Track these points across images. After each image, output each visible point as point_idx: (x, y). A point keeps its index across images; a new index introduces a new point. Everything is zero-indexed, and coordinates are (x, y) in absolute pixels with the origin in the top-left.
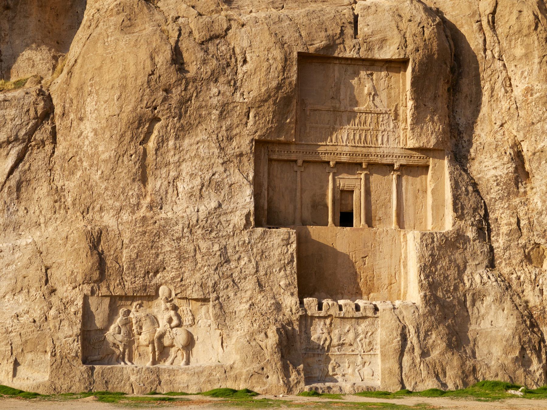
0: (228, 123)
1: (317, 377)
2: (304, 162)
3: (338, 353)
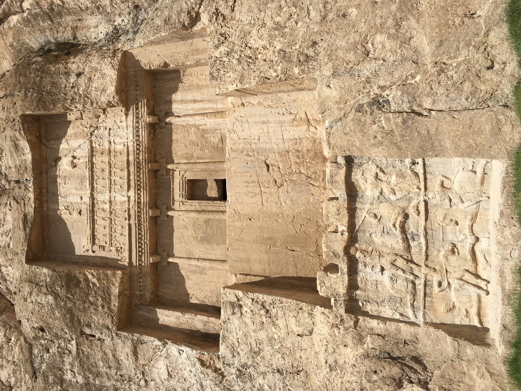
0: (101, 364)
2: (155, 252)
3: (423, 240)
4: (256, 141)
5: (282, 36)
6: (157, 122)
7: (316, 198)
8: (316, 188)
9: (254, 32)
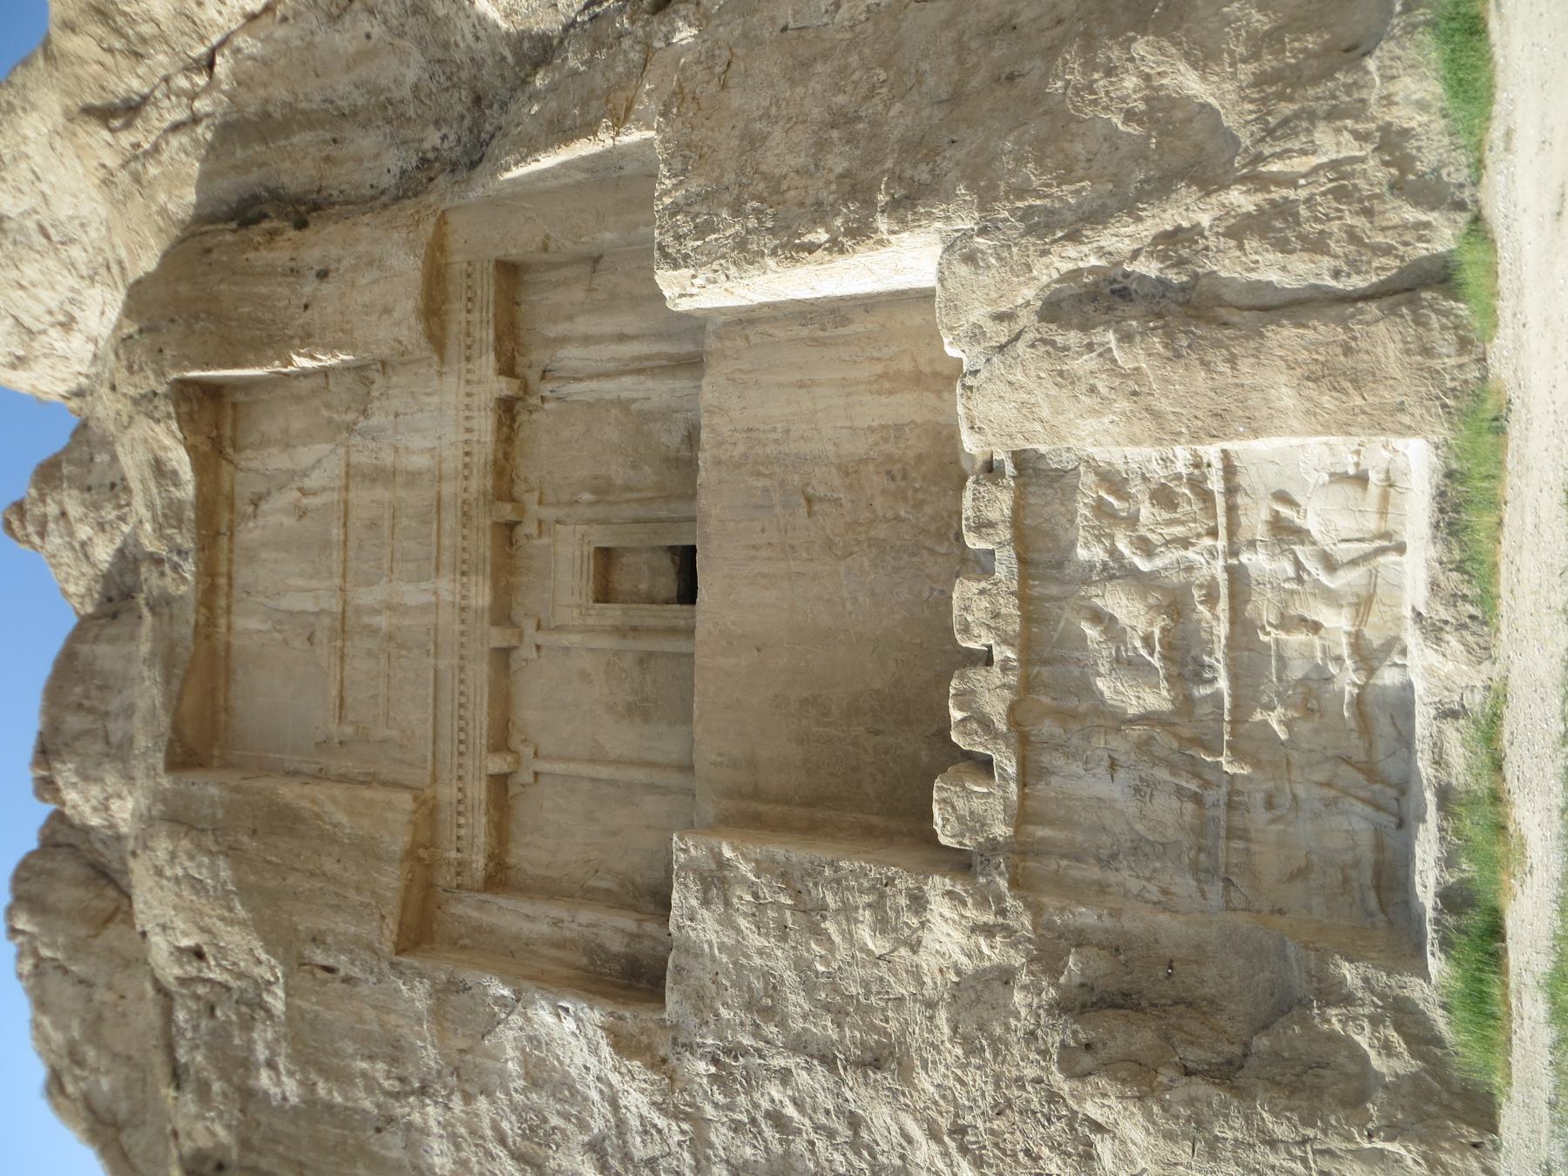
1: (1378, 831)
2: (500, 742)
4: (779, 436)
5: (848, 142)
6: (521, 394)
7: (938, 587)
8: (940, 560)
9: (778, 134)
